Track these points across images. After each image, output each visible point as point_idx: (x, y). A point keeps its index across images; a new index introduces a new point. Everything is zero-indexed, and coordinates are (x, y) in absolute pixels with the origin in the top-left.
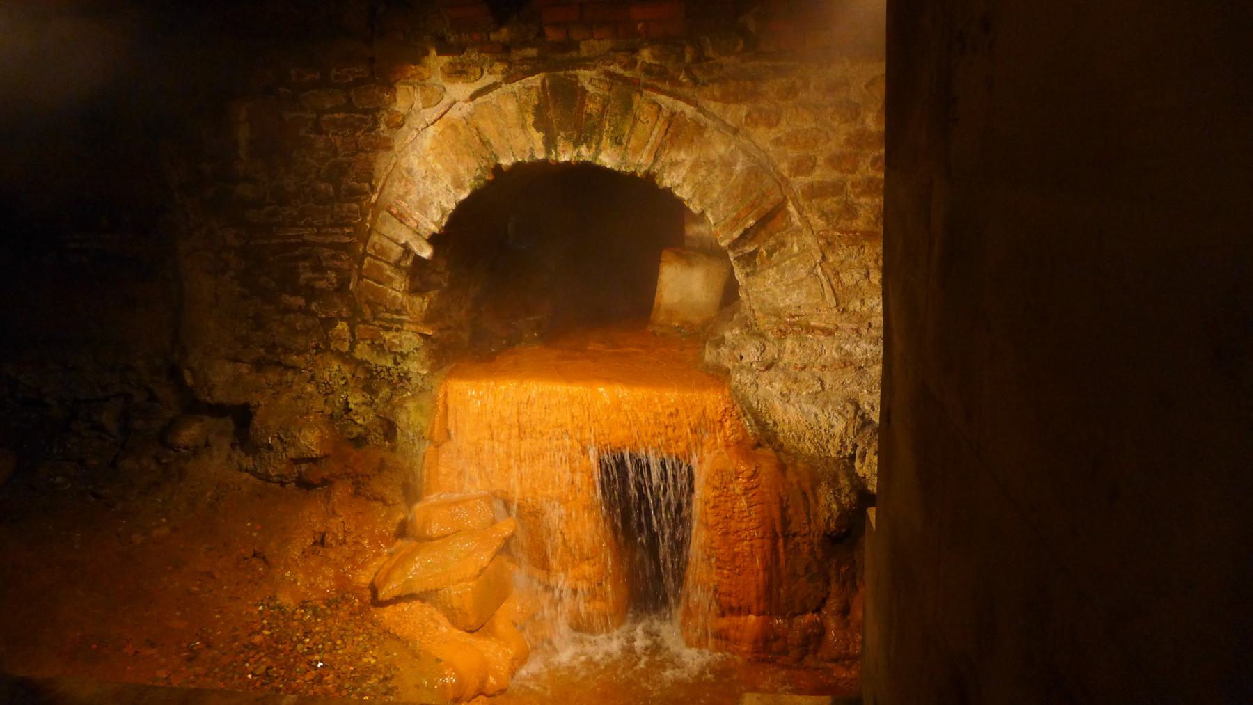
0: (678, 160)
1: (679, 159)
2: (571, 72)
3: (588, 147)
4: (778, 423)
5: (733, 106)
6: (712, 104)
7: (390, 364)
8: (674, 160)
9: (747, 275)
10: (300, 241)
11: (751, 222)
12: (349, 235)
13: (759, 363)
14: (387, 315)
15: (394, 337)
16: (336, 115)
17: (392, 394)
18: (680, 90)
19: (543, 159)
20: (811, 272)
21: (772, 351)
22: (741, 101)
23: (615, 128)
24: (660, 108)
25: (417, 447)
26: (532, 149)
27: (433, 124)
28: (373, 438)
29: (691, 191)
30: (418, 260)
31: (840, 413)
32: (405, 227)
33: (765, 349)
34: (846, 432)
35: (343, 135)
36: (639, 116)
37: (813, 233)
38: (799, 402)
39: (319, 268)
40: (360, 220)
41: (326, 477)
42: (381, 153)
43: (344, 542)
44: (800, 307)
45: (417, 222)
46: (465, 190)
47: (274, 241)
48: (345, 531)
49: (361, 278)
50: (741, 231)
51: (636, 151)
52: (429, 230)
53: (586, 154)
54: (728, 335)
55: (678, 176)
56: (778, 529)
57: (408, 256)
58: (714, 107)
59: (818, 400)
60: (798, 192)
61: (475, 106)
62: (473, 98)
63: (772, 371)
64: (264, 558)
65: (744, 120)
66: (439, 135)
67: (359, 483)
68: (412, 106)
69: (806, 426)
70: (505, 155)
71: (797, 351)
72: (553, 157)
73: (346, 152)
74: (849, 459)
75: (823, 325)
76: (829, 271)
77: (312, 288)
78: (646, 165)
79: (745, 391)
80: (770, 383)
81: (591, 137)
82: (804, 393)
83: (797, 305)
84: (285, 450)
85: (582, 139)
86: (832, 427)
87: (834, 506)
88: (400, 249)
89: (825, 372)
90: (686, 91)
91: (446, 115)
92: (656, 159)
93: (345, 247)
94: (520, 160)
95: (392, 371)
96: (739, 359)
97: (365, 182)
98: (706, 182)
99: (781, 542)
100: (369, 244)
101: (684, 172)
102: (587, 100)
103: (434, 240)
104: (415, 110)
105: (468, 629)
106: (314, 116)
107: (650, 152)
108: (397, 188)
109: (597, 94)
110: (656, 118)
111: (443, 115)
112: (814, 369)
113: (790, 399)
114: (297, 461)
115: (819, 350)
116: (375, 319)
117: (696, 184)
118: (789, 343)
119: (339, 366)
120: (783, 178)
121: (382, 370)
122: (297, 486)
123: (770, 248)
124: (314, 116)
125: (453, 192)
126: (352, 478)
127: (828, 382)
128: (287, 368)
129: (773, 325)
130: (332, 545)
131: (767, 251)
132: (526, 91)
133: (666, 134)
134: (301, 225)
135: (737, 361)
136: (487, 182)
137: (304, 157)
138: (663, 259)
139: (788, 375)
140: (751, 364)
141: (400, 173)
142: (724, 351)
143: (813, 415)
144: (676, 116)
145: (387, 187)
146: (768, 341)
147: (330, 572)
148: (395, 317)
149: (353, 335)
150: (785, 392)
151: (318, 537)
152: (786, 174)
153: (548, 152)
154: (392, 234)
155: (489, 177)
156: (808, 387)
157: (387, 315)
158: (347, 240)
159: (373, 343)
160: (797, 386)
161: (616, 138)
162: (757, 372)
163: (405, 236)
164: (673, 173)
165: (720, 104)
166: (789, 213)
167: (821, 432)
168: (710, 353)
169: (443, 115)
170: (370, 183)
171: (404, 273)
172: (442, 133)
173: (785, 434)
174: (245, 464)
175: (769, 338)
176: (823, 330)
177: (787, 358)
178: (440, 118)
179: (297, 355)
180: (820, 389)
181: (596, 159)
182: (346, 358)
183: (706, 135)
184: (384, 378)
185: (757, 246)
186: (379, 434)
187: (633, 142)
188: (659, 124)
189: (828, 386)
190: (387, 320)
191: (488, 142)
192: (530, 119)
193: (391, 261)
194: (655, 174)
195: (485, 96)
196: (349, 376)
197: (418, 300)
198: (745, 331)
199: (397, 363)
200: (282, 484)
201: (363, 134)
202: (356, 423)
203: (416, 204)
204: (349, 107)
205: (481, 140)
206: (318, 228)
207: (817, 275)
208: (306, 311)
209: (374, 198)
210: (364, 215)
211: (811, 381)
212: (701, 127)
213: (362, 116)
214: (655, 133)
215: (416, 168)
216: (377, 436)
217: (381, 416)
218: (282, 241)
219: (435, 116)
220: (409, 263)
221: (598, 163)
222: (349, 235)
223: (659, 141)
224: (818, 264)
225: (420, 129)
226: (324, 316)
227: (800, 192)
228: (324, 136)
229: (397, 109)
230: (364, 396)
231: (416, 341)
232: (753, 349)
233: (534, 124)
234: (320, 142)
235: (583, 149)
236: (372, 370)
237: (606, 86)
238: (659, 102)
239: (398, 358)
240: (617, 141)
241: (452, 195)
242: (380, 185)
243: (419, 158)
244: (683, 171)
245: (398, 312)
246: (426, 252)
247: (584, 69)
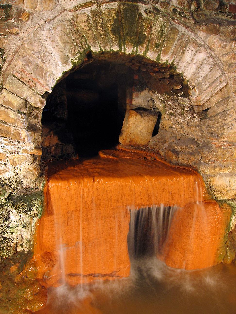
2: (135, 4)
51: (166, 53)
53: (141, 51)
104: (37, 11)
169: (56, 17)
193: (15, 109)
247: (143, 3)
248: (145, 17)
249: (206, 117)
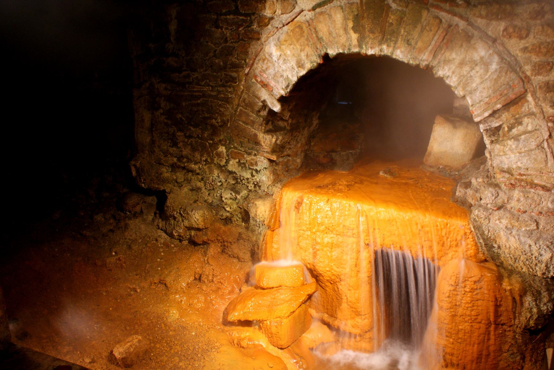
0: (450, 59)
1: (451, 58)
3: (388, 46)
4: (501, 248)
5: (494, 23)
6: (479, 20)
7: (249, 176)
8: (447, 58)
9: (492, 142)
10: (201, 94)
11: (499, 106)
13: (493, 205)
16: (228, 17)
17: (248, 195)
18: (456, 10)
19: (357, 52)
21: (503, 197)
22: (501, 19)
23: (408, 33)
24: (441, 21)
25: (261, 228)
27: (287, 24)
28: (235, 219)
29: (457, 81)
30: (271, 112)
31: (548, 247)
33: (498, 195)
34: (551, 260)
35: (231, 29)
36: (426, 26)
37: (544, 118)
38: (519, 235)
41: (205, 241)
43: (213, 281)
44: (527, 169)
46: (304, 68)
48: (213, 275)
50: (490, 112)
51: (421, 51)
52: (279, 93)
53: (386, 50)
54: (473, 181)
55: (449, 70)
56: (492, 319)
57: (265, 109)
58: (480, 22)
59: (533, 235)
60: (536, 87)
61: (315, 15)
62: (314, 9)
63: (502, 211)
64: (165, 284)
65: (501, 33)
66: (290, 32)
67: (225, 246)
68: (275, 12)
69: (522, 252)
70: (332, 48)
71: (522, 199)
73: (232, 41)
74: (550, 279)
75: (543, 183)
78: (427, 60)
79: (480, 222)
80: (499, 219)
81: (390, 39)
82: (523, 229)
83: (525, 167)
84: (183, 221)
85: (384, 40)
86: (541, 255)
87: (535, 310)
89: (541, 217)
90: (461, 10)
91: (296, 20)
92: (435, 56)
94: (341, 51)
95: (250, 180)
96: (479, 199)
98: (469, 75)
99: (492, 328)
101: (454, 67)
102: (390, 14)
103: (282, 100)
105: (280, 347)
106: (215, 17)
107: (431, 52)
109: (398, 10)
110: (437, 28)
111: (294, 19)
112: (533, 214)
113: (512, 232)
114: (190, 228)
115: (538, 201)
117: (461, 76)
118: (516, 194)
119: (218, 174)
120: (526, 77)
121: (244, 179)
122: (189, 243)
123: (510, 126)
124: (215, 17)
125: (296, 70)
126: (221, 242)
127: (542, 224)
129: (506, 180)
130: (205, 282)
131: (508, 127)
132: (349, 5)
133: (443, 39)
134: (203, 84)
135: (478, 201)
137: (207, 42)
138: (436, 121)
139: (513, 215)
140: (487, 204)
141: (264, 55)
142: (470, 192)
143: (528, 246)
144: (452, 28)
146: (501, 190)
147: (202, 298)
150: (509, 226)
151: (197, 276)
152: (529, 73)
156: (526, 226)
159: (239, 161)
160: (519, 224)
161: (408, 41)
162: (491, 210)
164: (446, 67)
165: (485, 20)
166: (528, 101)
167: (532, 258)
168: (460, 191)
169: (294, 19)
172: (292, 31)
173: (505, 255)
174: (160, 225)
175: (502, 188)
176: (544, 188)
177: (513, 204)
178: (292, 21)
179: (194, 164)
180: (535, 228)
181: (392, 54)
184: (244, 184)
185: (501, 123)
186: (239, 218)
187: (420, 44)
188: (440, 32)
189: (541, 227)
191: (322, 38)
192: (351, 24)
194: (433, 67)
195: (323, 8)
196: (223, 180)
197: (268, 137)
198: (486, 180)
199: (253, 176)
200: (181, 241)
201: (243, 29)
202: (226, 210)
204: (236, 12)
205: (317, 37)
206: (212, 87)
207: (543, 148)
211: (530, 222)
212: (469, 36)
213: (244, 18)
214: (436, 38)
216: (238, 219)
217: (241, 207)
219: (289, 20)
221: (394, 57)
223: (438, 44)
224: (545, 141)
225: (279, 28)
227: (538, 87)
228: (220, 30)
229: (265, 14)
230: (231, 194)
231: (266, 163)
232: (490, 195)
233: (353, 28)
234: (218, 33)
236: (238, 178)
237: (404, 4)
238: (440, 17)
239: (254, 173)
241: (295, 72)
244: (453, 67)
246: (277, 108)
248: (394, 8)
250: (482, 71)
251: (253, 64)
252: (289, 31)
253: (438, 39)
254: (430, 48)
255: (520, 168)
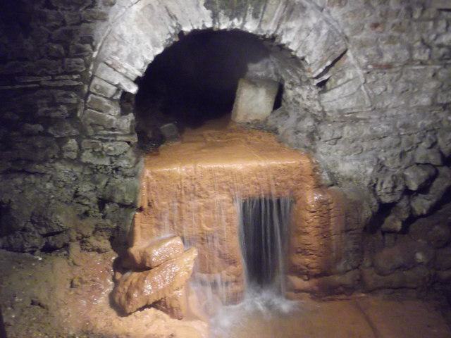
1: (291, 27)
12: (77, 80)
14: (105, 132)
15: (110, 146)
20: (359, 89)
26: (203, 21)
30: (125, 94)
32: (118, 74)
39: (54, 104)
40: (84, 69)
42: (99, 22)
45: (127, 70)
46: (159, 47)
47: (17, 87)
49: (86, 108)
50: (324, 67)
51: (267, 22)
53: (237, 24)
72: (217, 26)
76: (367, 87)
77: (49, 117)
81: (239, 13)
88: (114, 88)
92: (278, 27)
93: (77, 89)
94: (196, 28)
97: (88, 43)
100: (93, 84)
103: (138, 81)
108: (113, 47)
116: (96, 135)
118: (346, 128)
128: (29, 173)
136: (175, 42)
137: (39, 26)
145: (104, 47)
148: (111, 132)
149: (80, 147)
153: (214, 22)
154: (109, 78)
155: (176, 39)
157: (105, 132)
158: (76, 83)
161: (255, 14)
163: (118, 79)
170: (91, 43)
171: (117, 103)
172: (142, 10)
176: (364, 119)
182: (77, 161)
183: (307, 12)
187: (265, 17)
188: (281, 4)
190: (105, 136)
194: (277, 36)
197: (125, 121)
199: (112, 162)
203: (126, 58)
205: (170, 15)
206: (52, 75)
208: (45, 134)
209: (95, 54)
210: (88, 66)
215: (126, 33)
218: (23, 86)
220: (118, 97)
222: (77, 80)
226: (58, 136)
233: (205, 5)
234: (51, 14)
235: (235, 20)
239: (113, 158)
240: (255, 16)
242: (99, 45)
243: (127, 26)
244: (293, 34)
245: (113, 129)
246: (133, 89)
249: (325, 91)
250: (315, 36)
251: (101, 48)
252: (138, 10)
253: (280, 11)
254: (274, 19)
255: (347, 109)
